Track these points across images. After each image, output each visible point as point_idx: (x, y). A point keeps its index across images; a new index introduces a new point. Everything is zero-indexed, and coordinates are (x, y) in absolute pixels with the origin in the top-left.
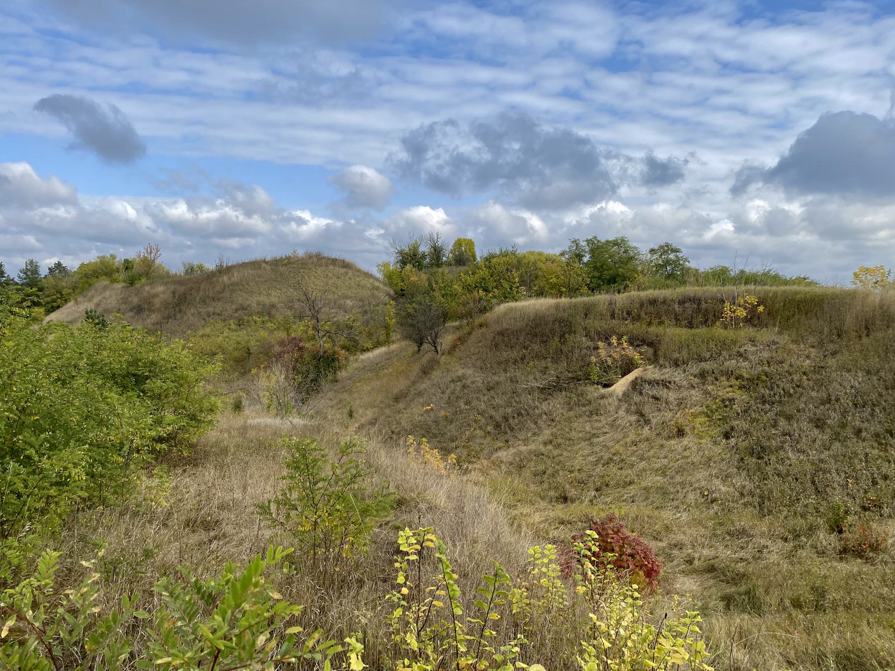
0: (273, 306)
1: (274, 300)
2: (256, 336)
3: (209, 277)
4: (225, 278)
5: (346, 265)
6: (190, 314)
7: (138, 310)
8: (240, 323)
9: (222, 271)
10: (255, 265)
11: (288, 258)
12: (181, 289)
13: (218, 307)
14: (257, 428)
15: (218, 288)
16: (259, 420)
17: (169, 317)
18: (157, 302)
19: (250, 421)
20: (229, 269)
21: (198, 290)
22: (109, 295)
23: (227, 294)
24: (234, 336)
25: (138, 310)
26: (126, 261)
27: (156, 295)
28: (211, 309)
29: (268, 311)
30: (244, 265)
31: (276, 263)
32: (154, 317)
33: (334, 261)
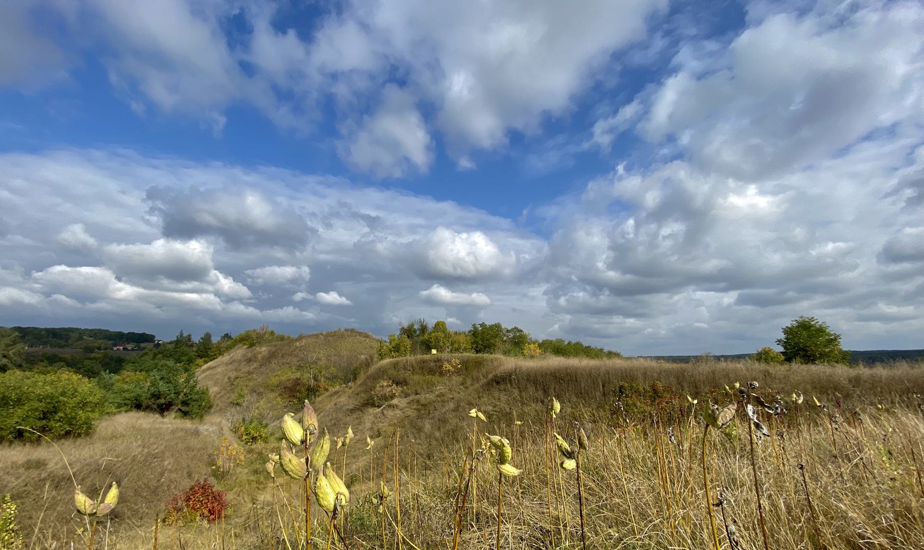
4: (298, 344)
5: (367, 336)
7: (249, 361)
10: (317, 336)
11: (335, 332)
12: (274, 349)
13: (289, 359)
15: (292, 349)
17: (262, 365)
18: (260, 356)
22: (240, 352)
25: (249, 361)
27: (260, 353)
30: (310, 336)
32: (255, 365)
33: (360, 334)
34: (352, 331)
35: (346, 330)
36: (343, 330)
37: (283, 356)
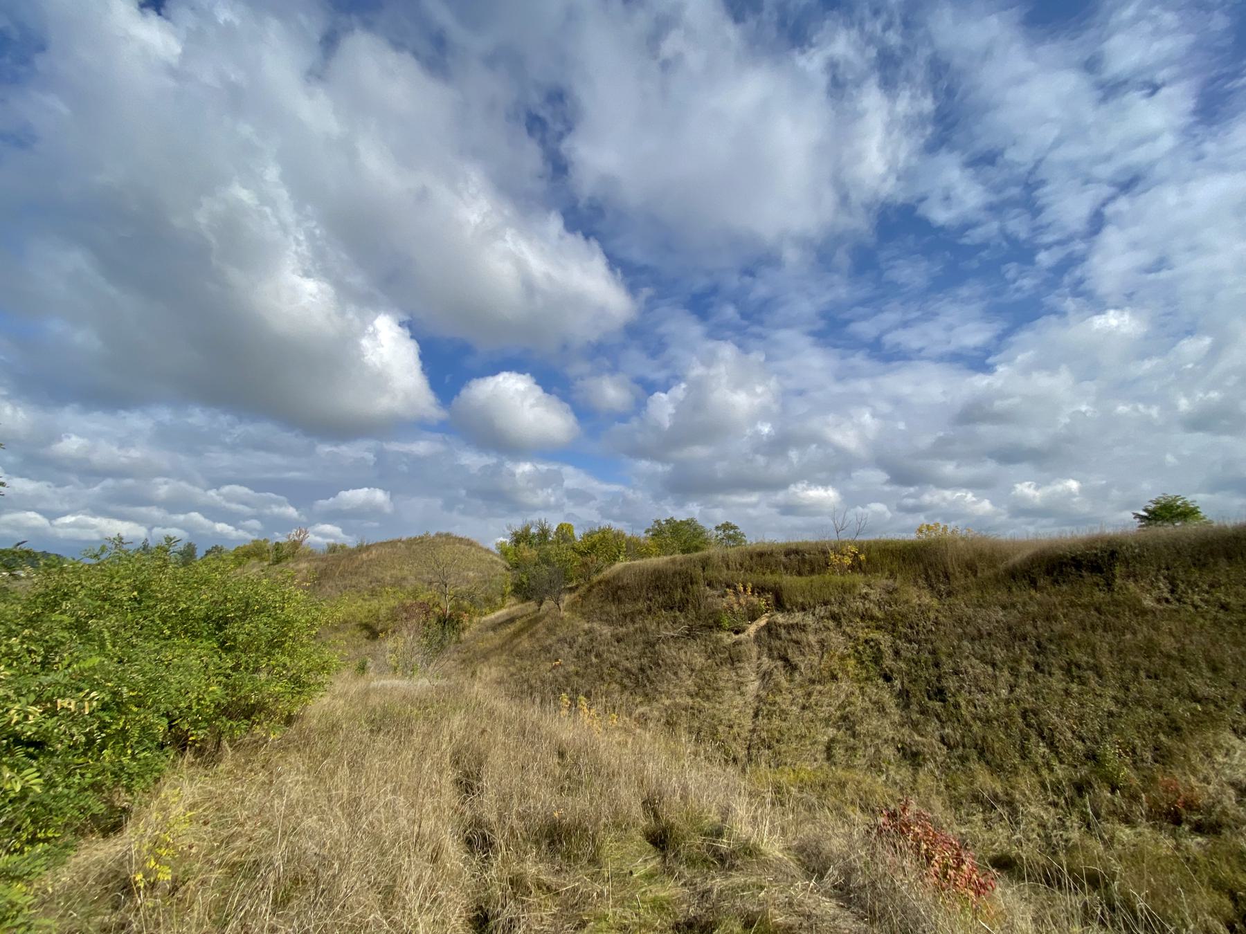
0: (404, 579)
1: (406, 572)
2: (384, 604)
3: (351, 554)
4: (364, 555)
6: (328, 586)
8: (373, 593)
9: (361, 549)
10: (392, 544)
14: (383, 691)
15: (357, 564)
16: (383, 682)
19: (374, 684)
20: (368, 548)
21: (338, 566)
23: (364, 569)
24: (366, 605)
26: (277, 543)
28: (347, 582)
29: (399, 583)
30: (382, 544)
31: (411, 543)
34: (448, 536)
35: (439, 535)
36: (432, 534)
37: (342, 575)
